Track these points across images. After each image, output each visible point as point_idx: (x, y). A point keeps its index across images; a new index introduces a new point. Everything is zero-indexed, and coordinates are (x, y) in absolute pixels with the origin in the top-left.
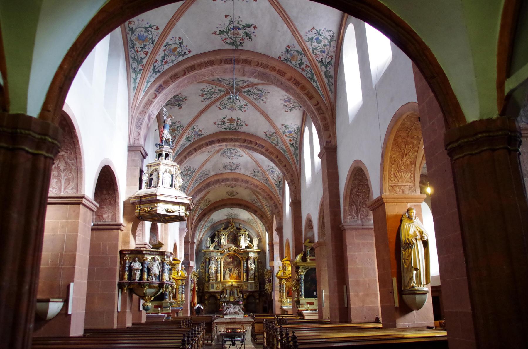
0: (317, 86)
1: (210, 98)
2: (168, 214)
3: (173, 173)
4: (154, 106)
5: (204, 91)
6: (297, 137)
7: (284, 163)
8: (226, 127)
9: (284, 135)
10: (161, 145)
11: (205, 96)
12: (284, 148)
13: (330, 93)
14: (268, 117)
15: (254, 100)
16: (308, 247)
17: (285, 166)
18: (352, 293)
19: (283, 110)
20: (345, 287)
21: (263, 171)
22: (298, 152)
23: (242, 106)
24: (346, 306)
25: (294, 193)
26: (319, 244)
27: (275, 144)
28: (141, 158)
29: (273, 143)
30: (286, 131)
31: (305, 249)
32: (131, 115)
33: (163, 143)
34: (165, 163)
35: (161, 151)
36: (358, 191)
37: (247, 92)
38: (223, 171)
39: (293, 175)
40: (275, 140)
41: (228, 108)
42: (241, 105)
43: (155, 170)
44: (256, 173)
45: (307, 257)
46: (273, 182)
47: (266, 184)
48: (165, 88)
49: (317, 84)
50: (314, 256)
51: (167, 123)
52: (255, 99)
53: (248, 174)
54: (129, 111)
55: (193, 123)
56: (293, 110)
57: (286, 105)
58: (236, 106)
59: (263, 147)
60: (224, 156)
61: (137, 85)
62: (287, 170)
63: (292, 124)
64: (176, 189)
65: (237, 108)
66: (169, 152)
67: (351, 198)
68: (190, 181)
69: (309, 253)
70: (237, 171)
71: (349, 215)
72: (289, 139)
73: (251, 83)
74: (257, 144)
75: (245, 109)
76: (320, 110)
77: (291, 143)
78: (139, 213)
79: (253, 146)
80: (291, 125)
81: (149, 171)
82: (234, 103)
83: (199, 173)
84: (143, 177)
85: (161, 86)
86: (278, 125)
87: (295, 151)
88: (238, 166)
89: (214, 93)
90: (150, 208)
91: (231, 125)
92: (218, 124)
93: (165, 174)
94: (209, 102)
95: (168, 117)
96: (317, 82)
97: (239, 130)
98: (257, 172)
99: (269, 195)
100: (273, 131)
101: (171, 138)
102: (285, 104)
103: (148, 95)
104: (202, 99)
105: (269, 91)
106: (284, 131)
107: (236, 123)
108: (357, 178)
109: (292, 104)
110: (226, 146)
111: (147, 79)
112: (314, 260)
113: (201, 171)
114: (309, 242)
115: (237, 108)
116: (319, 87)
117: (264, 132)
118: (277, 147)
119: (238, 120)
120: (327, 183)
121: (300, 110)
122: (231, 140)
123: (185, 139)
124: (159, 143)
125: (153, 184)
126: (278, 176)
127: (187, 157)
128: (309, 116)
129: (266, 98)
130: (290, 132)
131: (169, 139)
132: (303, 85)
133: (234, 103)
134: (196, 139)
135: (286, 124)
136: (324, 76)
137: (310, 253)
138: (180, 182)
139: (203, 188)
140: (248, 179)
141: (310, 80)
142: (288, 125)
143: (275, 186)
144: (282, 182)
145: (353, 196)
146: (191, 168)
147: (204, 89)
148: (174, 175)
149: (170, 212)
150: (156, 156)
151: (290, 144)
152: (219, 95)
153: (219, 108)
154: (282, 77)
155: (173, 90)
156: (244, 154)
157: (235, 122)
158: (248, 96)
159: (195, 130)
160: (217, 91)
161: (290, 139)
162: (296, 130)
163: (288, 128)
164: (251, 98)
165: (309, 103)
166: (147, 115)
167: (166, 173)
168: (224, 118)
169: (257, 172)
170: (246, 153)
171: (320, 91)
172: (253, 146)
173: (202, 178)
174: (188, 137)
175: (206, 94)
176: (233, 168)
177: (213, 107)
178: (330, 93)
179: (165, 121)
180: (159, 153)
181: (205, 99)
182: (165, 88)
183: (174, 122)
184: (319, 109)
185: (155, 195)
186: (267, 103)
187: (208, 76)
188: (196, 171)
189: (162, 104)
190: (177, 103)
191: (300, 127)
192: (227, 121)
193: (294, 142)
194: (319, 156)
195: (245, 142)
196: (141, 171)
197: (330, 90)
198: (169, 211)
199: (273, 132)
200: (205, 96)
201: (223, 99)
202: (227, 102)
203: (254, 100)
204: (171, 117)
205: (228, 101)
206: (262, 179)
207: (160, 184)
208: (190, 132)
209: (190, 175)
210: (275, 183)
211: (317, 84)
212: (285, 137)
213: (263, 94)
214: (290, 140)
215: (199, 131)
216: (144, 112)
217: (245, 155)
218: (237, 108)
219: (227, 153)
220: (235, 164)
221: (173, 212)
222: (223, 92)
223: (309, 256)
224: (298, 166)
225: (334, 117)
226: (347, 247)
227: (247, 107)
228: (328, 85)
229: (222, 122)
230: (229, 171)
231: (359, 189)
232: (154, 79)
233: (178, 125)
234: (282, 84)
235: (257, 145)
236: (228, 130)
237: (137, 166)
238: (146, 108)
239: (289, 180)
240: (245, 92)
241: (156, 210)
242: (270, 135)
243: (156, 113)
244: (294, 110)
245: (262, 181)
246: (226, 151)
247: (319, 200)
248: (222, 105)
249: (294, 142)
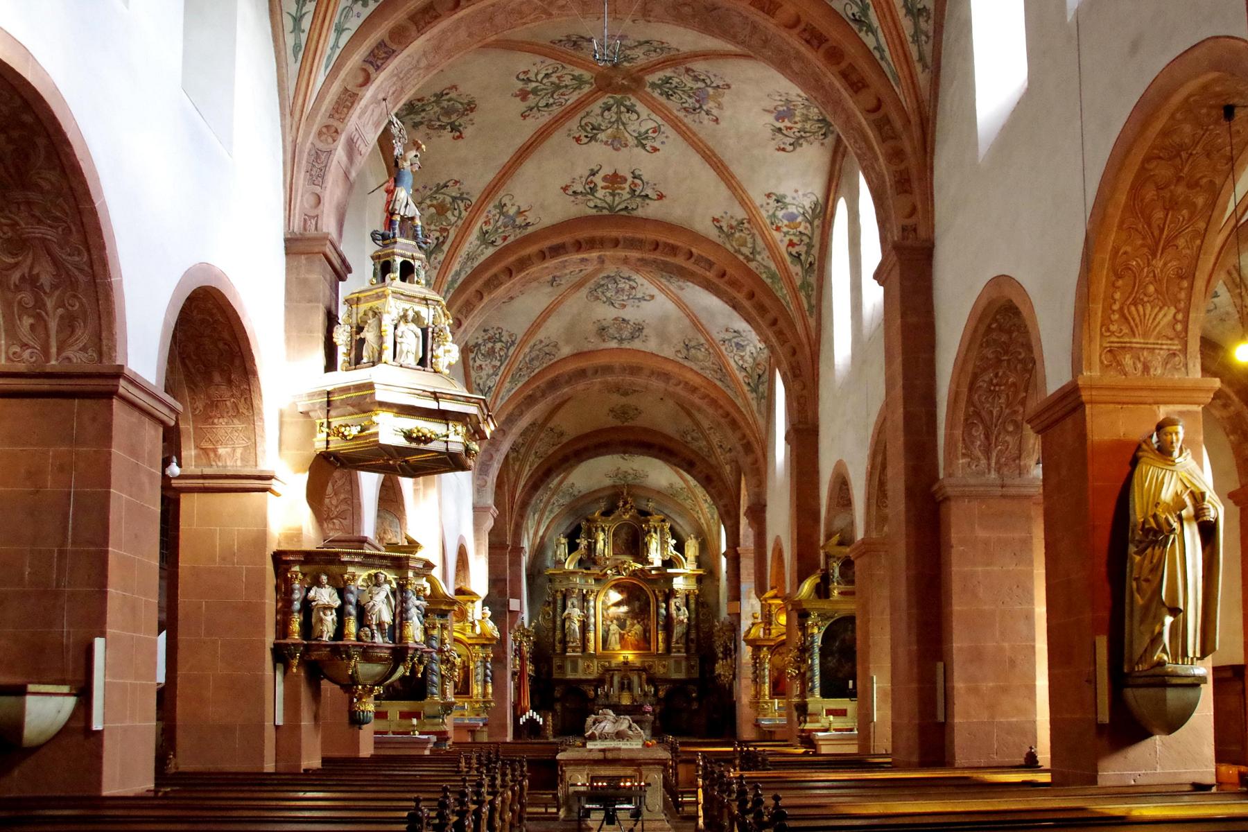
0: (879, 48)
1: (547, 105)
2: (414, 445)
3: (426, 322)
4: (363, 112)
5: (529, 80)
6: (813, 234)
7: (773, 313)
8: (599, 203)
9: (774, 227)
10: (388, 238)
11: (531, 96)
12: (773, 266)
13: (918, 67)
14: (726, 168)
15: (681, 114)
16: (834, 557)
17: (774, 323)
18: (959, 685)
19: (770, 149)
20: (940, 665)
21: (711, 342)
22: (812, 279)
23: (647, 132)
24: (941, 718)
25: (799, 403)
26: (868, 547)
27: (746, 257)
28: (328, 277)
29: (739, 251)
30: (780, 214)
31: (827, 563)
32: (289, 139)
33: (397, 231)
34: (401, 291)
35: (388, 255)
36: (995, 381)
37: (659, 86)
38: (595, 343)
39: (798, 350)
40: (744, 244)
41: (605, 139)
42: (643, 130)
43: (370, 314)
44: (693, 351)
45: (831, 586)
46: (740, 376)
47: (719, 383)
48: (394, 51)
49: (877, 40)
50: (852, 582)
51: (406, 165)
52: (685, 109)
53: (668, 352)
54: (283, 127)
55: (499, 189)
56: (801, 145)
57: (780, 130)
58: (626, 134)
59: (710, 264)
60: (597, 298)
61: (304, 37)
62: (780, 334)
63: (796, 191)
64: (435, 372)
65: (630, 138)
66: (413, 258)
67: (970, 402)
68: (500, 374)
69: (837, 574)
70: (637, 345)
71: (964, 455)
72: (786, 240)
73: (672, 53)
74: (691, 254)
75: (655, 144)
76: (887, 127)
77: (794, 253)
78: (328, 442)
79: (680, 261)
80: (795, 195)
81: (354, 316)
82: (624, 124)
83: (527, 350)
84: (334, 335)
85: (381, 44)
86: (758, 198)
87: (804, 278)
88: (639, 329)
89: (558, 87)
90: (359, 428)
91: (613, 195)
92: (574, 192)
93: (402, 327)
94: (544, 118)
95: (406, 148)
96: (879, 30)
97: (640, 213)
98: (693, 347)
99: (728, 414)
100: (740, 214)
101: (418, 213)
102: (779, 125)
103: (342, 74)
104: (522, 106)
105: (728, 81)
106: (774, 215)
107: (628, 189)
108: (995, 340)
109: (799, 126)
110: (601, 260)
111: (336, 20)
112: (852, 593)
113: (531, 343)
114: (840, 544)
115: (630, 138)
116: (886, 49)
117: (714, 220)
118: (752, 265)
119: (637, 181)
120: (899, 360)
121: (822, 144)
122: (616, 243)
123: (478, 238)
124: (381, 230)
125: (365, 353)
126: (754, 359)
127: (485, 295)
128: (852, 160)
129: (720, 106)
130: (791, 218)
131: (412, 219)
132: (834, 44)
133: (624, 124)
134: (511, 239)
135: (781, 191)
136: (901, 12)
137: (841, 574)
138: (449, 351)
139: (539, 394)
140: (669, 368)
141: (855, 27)
142: (784, 197)
143: (746, 388)
144: (765, 378)
145: (976, 396)
146: (504, 333)
148: (430, 330)
149: (418, 440)
150: (375, 269)
151: (790, 254)
152: (574, 98)
153: (578, 140)
154: (768, 17)
155: (424, 63)
156: (655, 292)
157: (627, 186)
158: (663, 99)
159: (505, 209)
160: (567, 80)
161: (791, 241)
162: (810, 211)
163: (785, 206)
164: (673, 105)
165: (850, 103)
166: (342, 139)
167: (406, 322)
168: (593, 173)
169: (693, 347)
170: (662, 290)
171: (889, 65)
172: (680, 261)
173: (536, 363)
174: (487, 232)
175: (535, 92)
176: (626, 334)
177: (558, 137)
178: (918, 67)
179: (400, 162)
180: (382, 260)
181: (531, 109)
182: (394, 51)
183: (441, 184)
184: (882, 125)
185: (370, 386)
186: (723, 124)
187: (532, 17)
188: (517, 342)
189: (390, 106)
190: (445, 120)
191: (820, 201)
192: (601, 184)
193: (802, 249)
194: (877, 276)
195: (655, 249)
196: (331, 320)
197: (921, 58)
198: (414, 435)
199: (739, 218)
201: (587, 109)
202: (600, 118)
203: (681, 114)
204: (418, 148)
205: (602, 115)
206: (707, 368)
207: (388, 355)
208: (490, 216)
209: (502, 353)
210: (746, 380)
211: (877, 40)
212: (776, 234)
213: (711, 91)
214: (791, 244)
215: (520, 213)
216: (330, 132)
217: (660, 297)
218: (632, 142)
219: (608, 289)
220: (631, 323)
221: (428, 440)
222: (588, 86)
223: (838, 583)
224: (812, 322)
225: (928, 150)
226: (954, 551)
227: (662, 138)
228: (913, 42)
229: (587, 187)
230: (613, 344)
231: (996, 375)
232: (360, 21)
233: (454, 194)
234: (766, 42)
235: (693, 260)
236: (605, 212)
237: (317, 300)
238: (337, 116)
239: (785, 366)
240: (653, 85)
241: (376, 434)
242: (732, 228)
243: (372, 137)
244: (805, 144)
245: (709, 375)
246: (602, 282)
247: (873, 418)
248: (586, 131)
249: (802, 249)
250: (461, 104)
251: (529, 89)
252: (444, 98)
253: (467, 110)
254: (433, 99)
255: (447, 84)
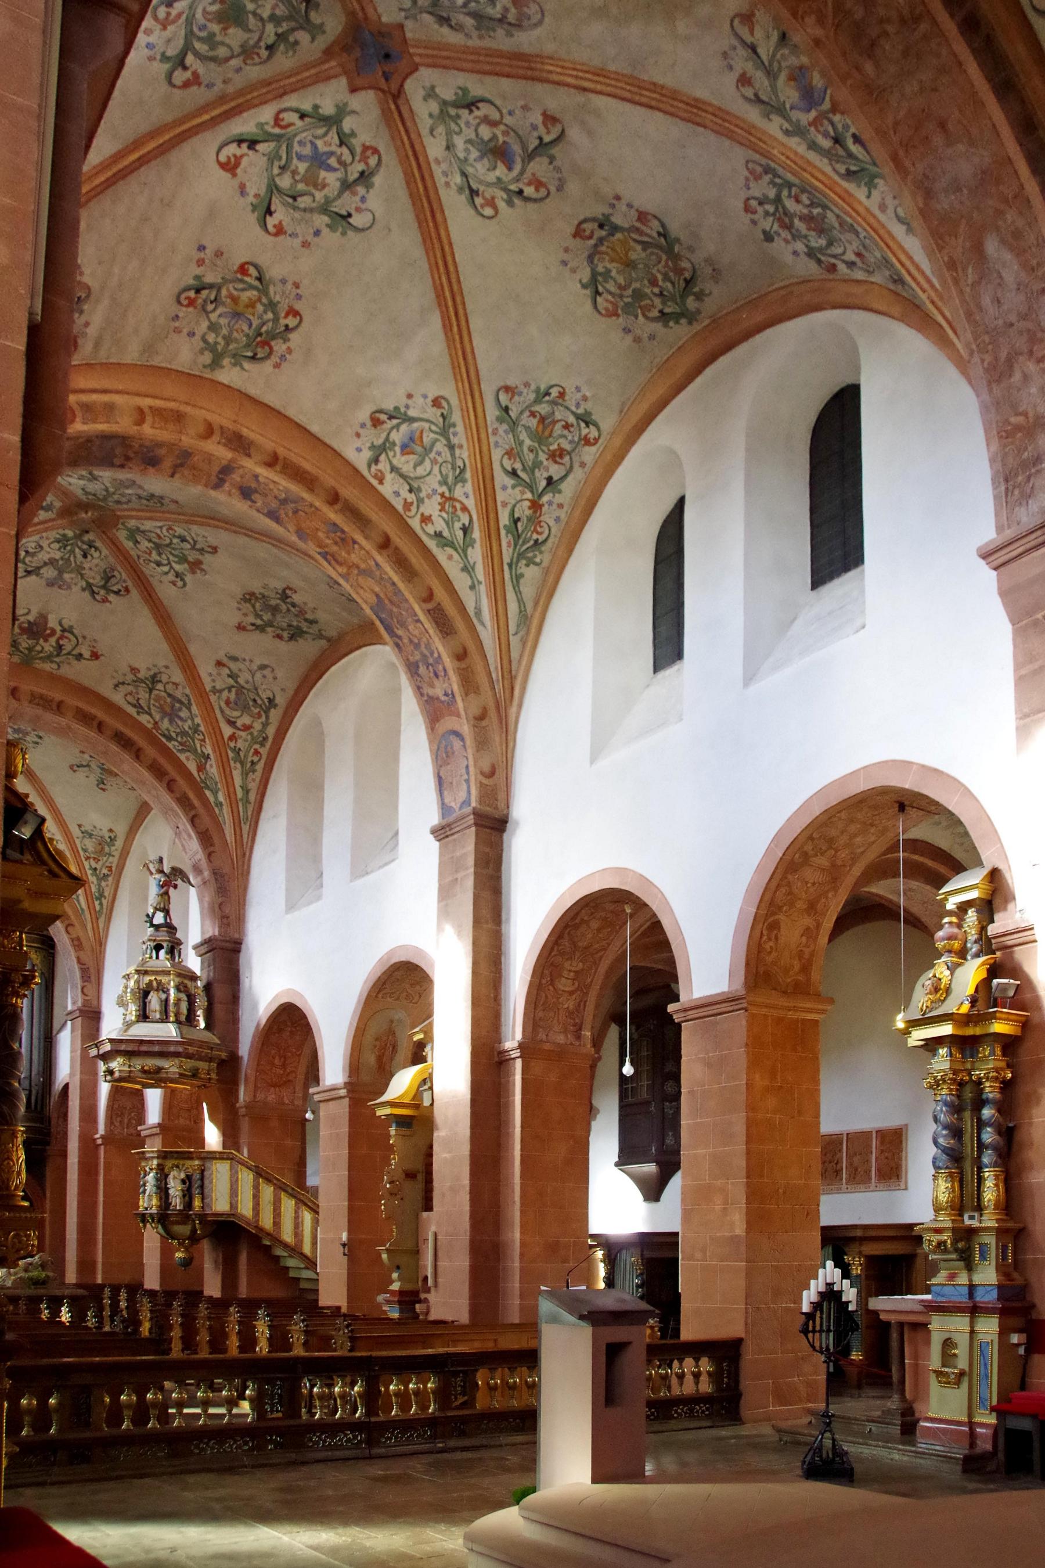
104: (207, 558)
147: (174, 583)
181: (202, 551)
190: (284, 607)
200: (190, 559)
246: (469, 22)
250: (254, 606)
251: (186, 566)
252: (259, 622)
253: (257, 598)
254: (269, 629)
255: (241, 637)
